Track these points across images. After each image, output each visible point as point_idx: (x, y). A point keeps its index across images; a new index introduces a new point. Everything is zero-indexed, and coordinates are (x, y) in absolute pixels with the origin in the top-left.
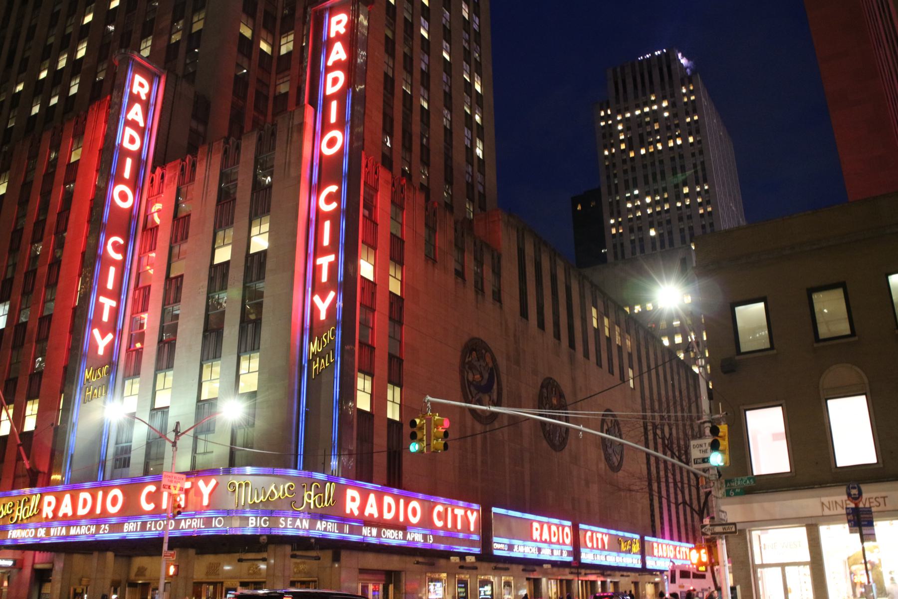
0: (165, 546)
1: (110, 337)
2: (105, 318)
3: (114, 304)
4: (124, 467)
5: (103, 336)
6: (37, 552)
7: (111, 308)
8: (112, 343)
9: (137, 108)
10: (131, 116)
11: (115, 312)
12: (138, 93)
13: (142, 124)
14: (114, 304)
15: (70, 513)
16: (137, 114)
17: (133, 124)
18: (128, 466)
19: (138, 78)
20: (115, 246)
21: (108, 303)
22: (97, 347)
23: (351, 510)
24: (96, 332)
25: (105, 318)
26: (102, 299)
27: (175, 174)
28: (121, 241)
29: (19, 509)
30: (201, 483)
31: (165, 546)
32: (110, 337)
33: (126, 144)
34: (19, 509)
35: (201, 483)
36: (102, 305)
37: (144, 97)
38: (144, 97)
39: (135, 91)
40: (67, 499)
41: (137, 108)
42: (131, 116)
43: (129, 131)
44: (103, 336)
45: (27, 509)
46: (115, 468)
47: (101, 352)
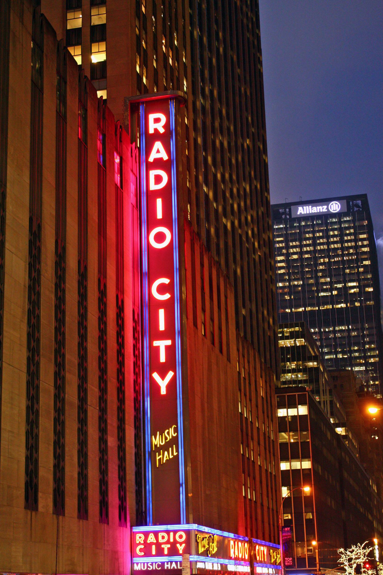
1: (170, 375)
2: (163, 359)
3: (169, 342)
5: (163, 377)
7: (167, 347)
8: (174, 380)
9: (158, 145)
10: (151, 159)
11: (170, 350)
12: (156, 130)
13: (166, 158)
14: (169, 342)
17: (158, 164)
19: (152, 117)
20: (162, 289)
22: (158, 388)
24: (155, 376)
25: (163, 359)
26: (156, 343)
28: (166, 281)
32: (170, 375)
33: (153, 187)
36: (158, 348)
37: (162, 131)
38: (162, 131)
39: (151, 131)
41: (158, 145)
42: (151, 159)
43: (153, 173)
44: (163, 377)
47: (163, 391)
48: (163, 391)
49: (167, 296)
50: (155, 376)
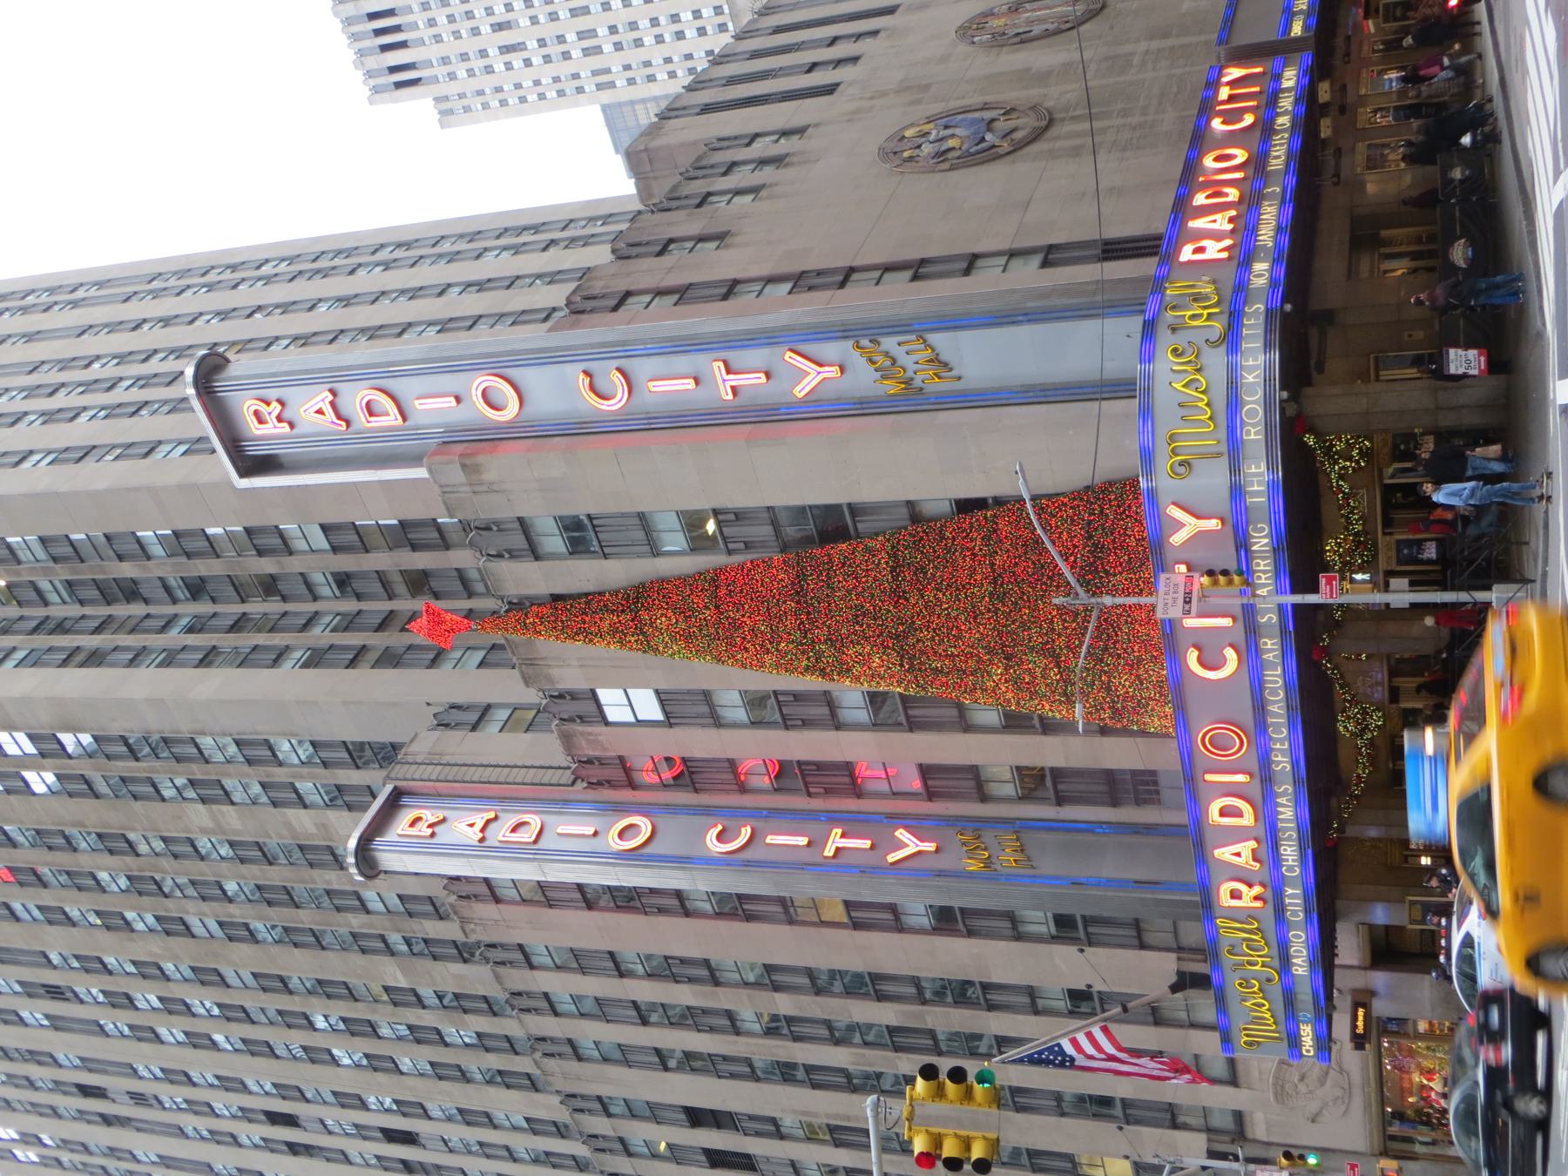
0: (1311, 599)
1: (901, 834)
4: (1156, 783)
6: (1337, 961)
15: (1252, 844)
16: (471, 825)
18: (1153, 773)
21: (835, 840)
23: (1220, 251)
27: (582, 734)
29: (1250, 964)
30: (1178, 539)
31: (1311, 599)
34: (1250, 964)
35: (1178, 539)
40: (1224, 853)
45: (1248, 947)
46: (1159, 802)
48: (930, 847)
49: (746, 832)
50: (891, 858)
